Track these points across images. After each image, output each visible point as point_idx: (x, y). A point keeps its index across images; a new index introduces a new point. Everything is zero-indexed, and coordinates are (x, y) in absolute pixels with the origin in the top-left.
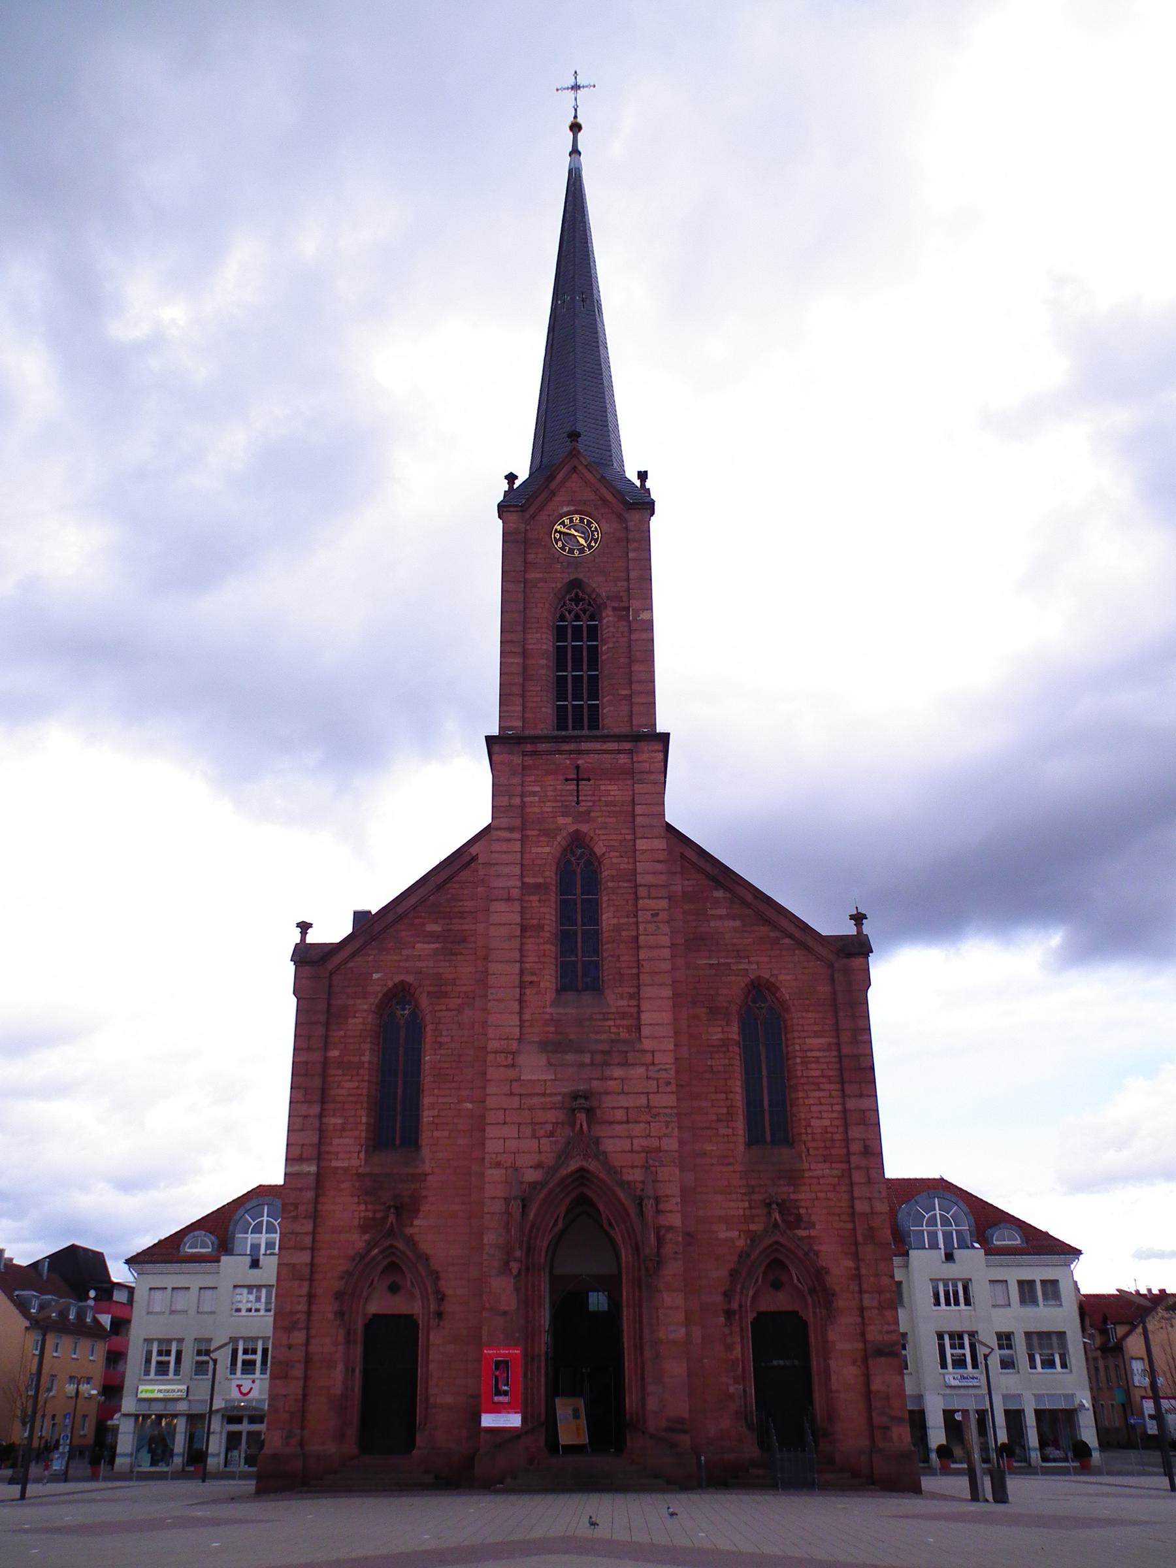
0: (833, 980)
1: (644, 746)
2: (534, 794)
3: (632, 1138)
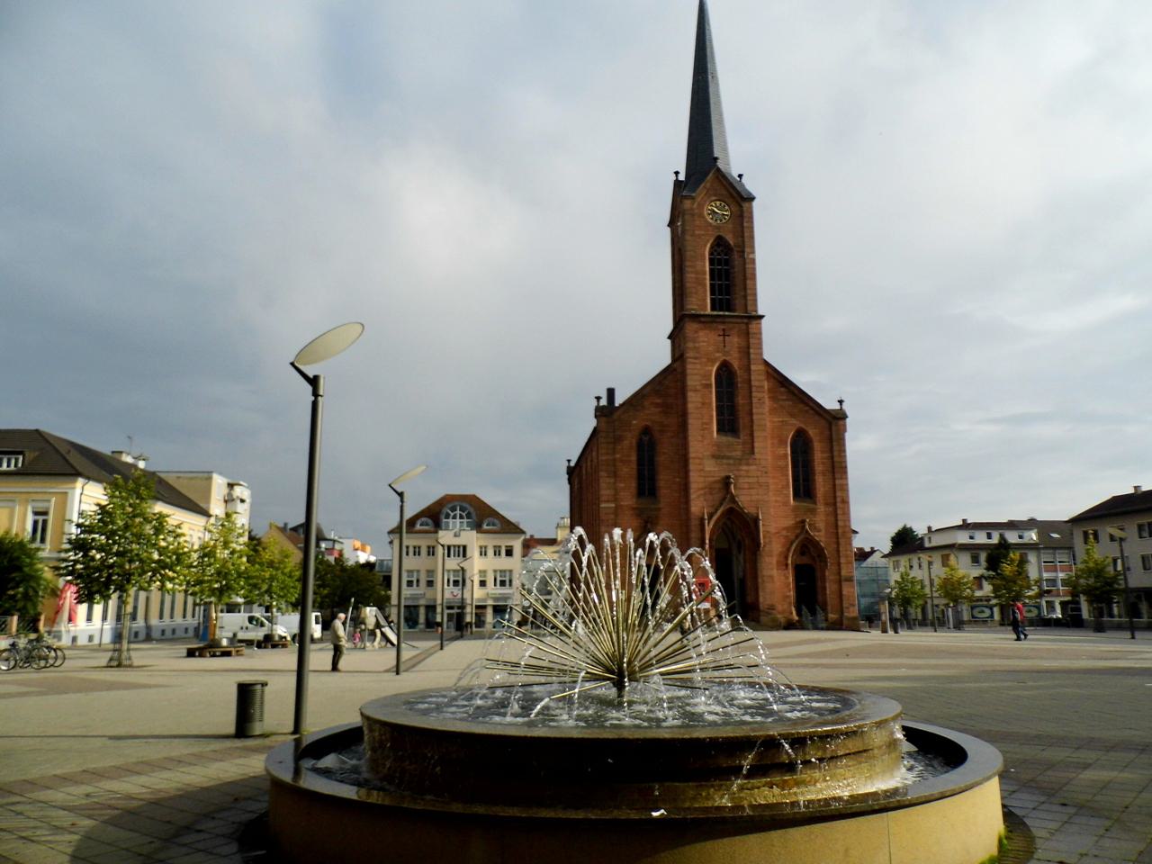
1: (755, 322)
2: (704, 342)
3: (751, 495)
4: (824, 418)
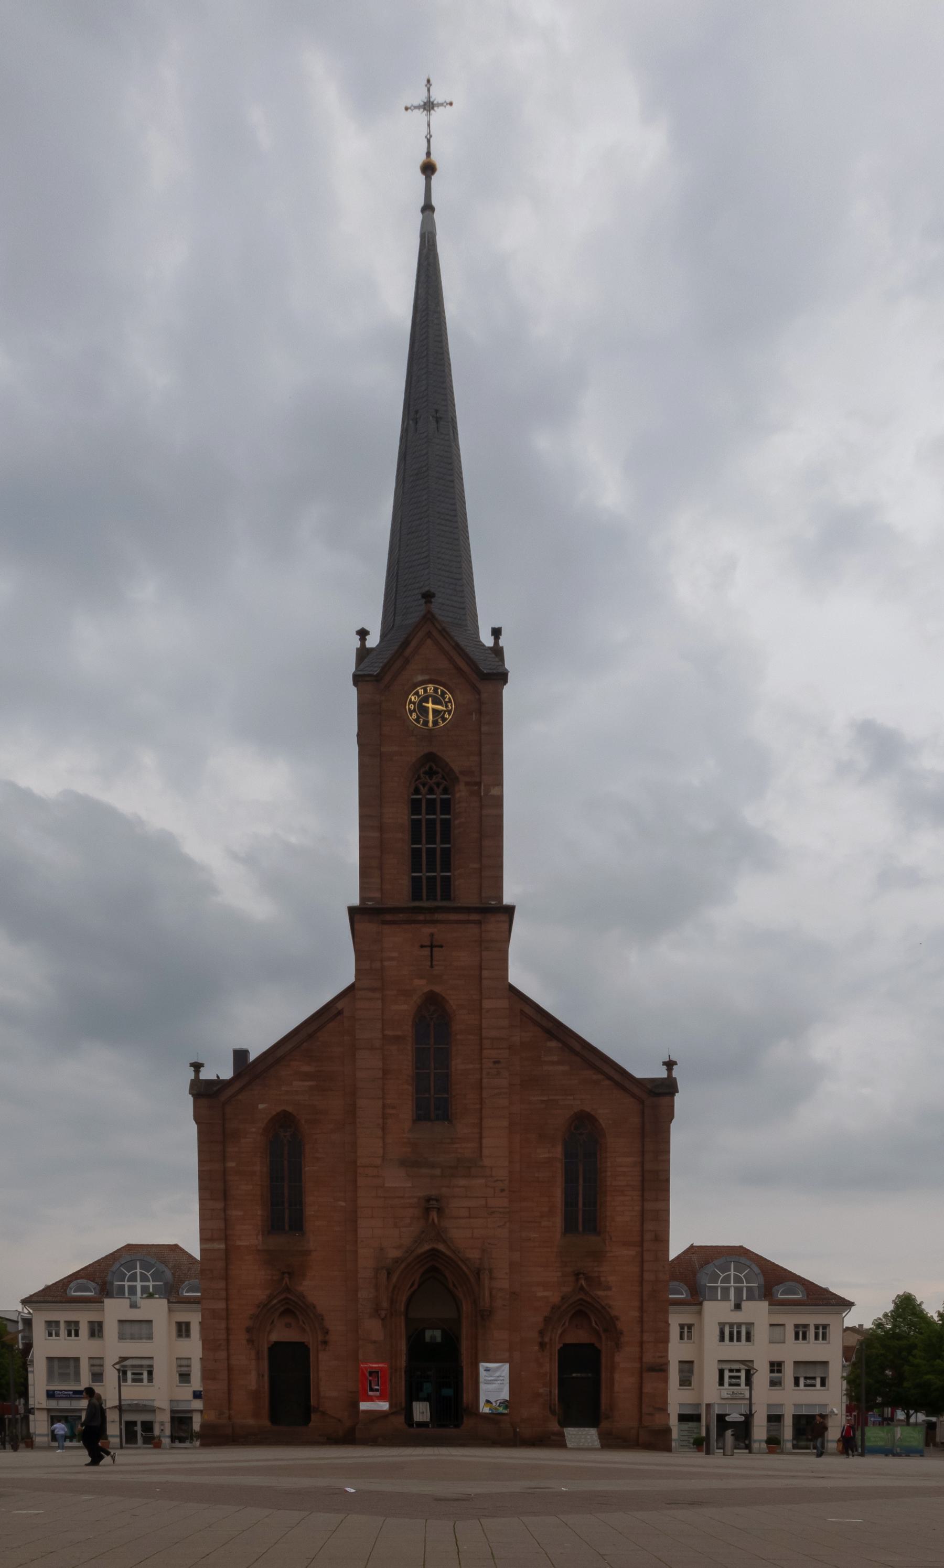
0: (643, 1113)
4: (633, 1095)
